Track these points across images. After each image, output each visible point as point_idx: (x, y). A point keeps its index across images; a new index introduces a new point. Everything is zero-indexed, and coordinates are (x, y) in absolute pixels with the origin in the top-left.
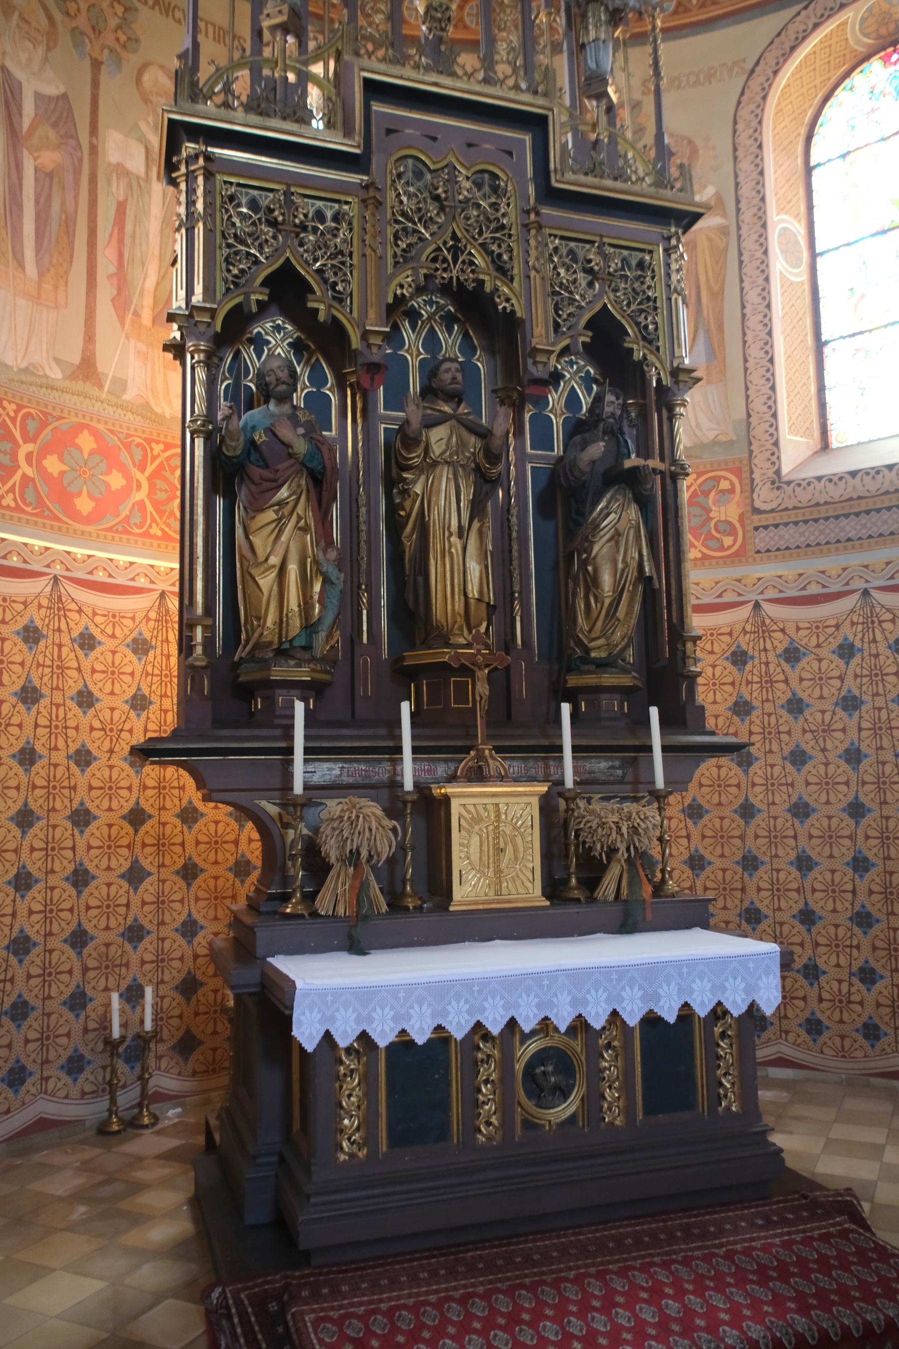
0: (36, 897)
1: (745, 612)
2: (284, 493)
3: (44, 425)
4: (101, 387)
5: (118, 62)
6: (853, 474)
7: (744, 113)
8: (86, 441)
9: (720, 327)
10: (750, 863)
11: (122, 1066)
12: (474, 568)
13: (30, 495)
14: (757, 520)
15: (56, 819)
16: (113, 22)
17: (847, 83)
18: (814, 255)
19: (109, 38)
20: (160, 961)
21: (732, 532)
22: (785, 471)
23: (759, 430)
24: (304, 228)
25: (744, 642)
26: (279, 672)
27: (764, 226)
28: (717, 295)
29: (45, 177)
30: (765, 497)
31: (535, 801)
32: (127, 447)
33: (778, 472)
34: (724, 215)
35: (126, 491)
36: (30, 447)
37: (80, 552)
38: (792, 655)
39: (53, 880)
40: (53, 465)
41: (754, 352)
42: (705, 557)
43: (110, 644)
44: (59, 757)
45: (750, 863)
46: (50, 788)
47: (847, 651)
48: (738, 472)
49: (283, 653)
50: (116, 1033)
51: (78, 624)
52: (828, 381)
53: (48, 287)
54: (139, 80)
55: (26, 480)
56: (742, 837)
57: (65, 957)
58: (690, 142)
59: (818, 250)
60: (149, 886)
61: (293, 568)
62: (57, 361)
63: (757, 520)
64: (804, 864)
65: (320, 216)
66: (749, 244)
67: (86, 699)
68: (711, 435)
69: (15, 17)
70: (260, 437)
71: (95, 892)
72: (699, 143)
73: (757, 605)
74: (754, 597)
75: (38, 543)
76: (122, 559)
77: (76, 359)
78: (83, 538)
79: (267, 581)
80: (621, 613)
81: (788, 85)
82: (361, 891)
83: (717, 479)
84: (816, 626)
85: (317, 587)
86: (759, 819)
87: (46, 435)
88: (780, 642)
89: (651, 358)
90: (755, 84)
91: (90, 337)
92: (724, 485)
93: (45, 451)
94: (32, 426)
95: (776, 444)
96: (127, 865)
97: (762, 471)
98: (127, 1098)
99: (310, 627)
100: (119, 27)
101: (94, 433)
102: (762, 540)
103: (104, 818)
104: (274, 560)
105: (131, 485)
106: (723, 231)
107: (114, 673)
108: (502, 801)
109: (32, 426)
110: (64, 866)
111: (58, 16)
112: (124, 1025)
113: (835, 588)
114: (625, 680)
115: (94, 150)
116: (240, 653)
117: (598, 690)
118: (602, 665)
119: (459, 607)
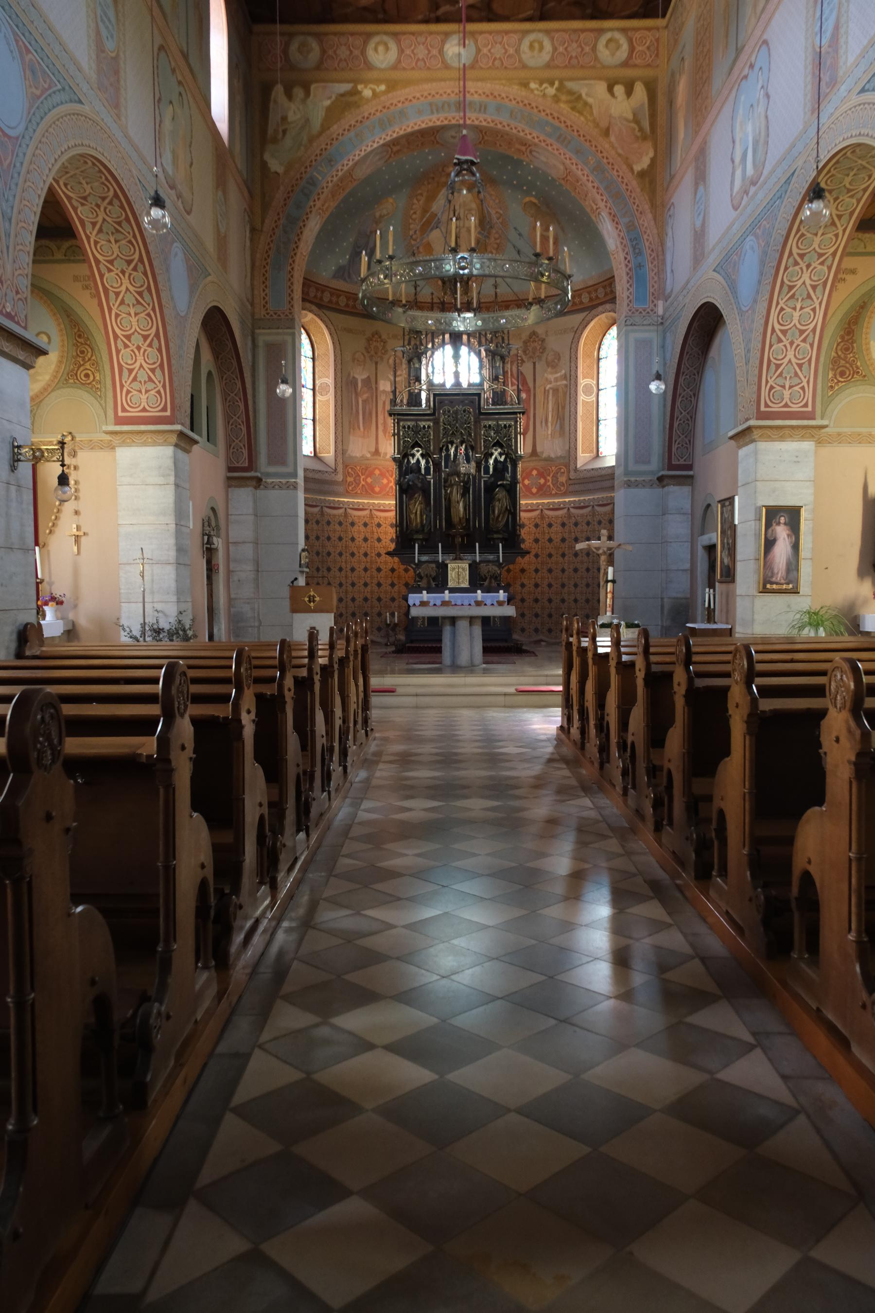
0: (369, 588)
1: (565, 511)
2: (416, 495)
3: (366, 470)
4: (380, 456)
5: (382, 358)
6: (593, 469)
7: (573, 346)
8: (377, 472)
9: (564, 420)
10: (563, 586)
11: (390, 632)
12: (461, 509)
13: (364, 490)
14: (571, 482)
15: (373, 570)
16: (381, 348)
17: (609, 332)
18: (598, 390)
19: (379, 354)
20: (399, 607)
21: (563, 485)
22: (578, 466)
23: (572, 453)
24: (420, 431)
25: (565, 520)
26: (415, 537)
27: (577, 386)
28: (564, 408)
29: (364, 402)
30: (572, 475)
31: (467, 565)
32: (388, 471)
33: (576, 467)
34: (566, 380)
35: (388, 483)
36: (363, 477)
37: (376, 502)
38: (576, 524)
39: (373, 585)
40: (369, 480)
41: (572, 428)
42: (556, 493)
43: (384, 525)
44: (373, 555)
45: (563, 586)
46: (371, 562)
47: (588, 523)
48: (566, 467)
49: (417, 532)
50: (388, 622)
51: (376, 521)
52: (600, 433)
53: (366, 432)
54: (388, 362)
55: (363, 485)
56: (562, 578)
57: (376, 603)
58: (559, 354)
59: (600, 387)
60: (396, 587)
61: (418, 512)
62: (369, 452)
63: (571, 482)
64: (576, 586)
65: (424, 427)
66: (572, 392)
67: (379, 540)
68: (560, 454)
69: (356, 361)
70: (410, 483)
71: (383, 588)
72: (561, 355)
73: (569, 509)
74: (567, 506)
75: (366, 501)
76: (387, 502)
77: (373, 450)
78: (377, 499)
79: (413, 516)
80: (500, 520)
81: (587, 336)
82: (429, 583)
83: (561, 469)
84: (582, 515)
85: (425, 517)
86: (566, 573)
87: (367, 472)
88: (573, 520)
89: (510, 452)
90: (577, 335)
91: (377, 443)
92: (562, 470)
93: (366, 478)
94: (364, 471)
95: (576, 458)
96: (390, 582)
97: (572, 467)
98: (392, 639)
99: (423, 526)
100: (382, 349)
101: (379, 470)
102: (571, 488)
103: (384, 570)
104: (414, 511)
105: (389, 481)
106: (566, 386)
107: (386, 533)
108: (460, 565)
109: (364, 471)
110: (375, 581)
111: (366, 354)
112: (390, 622)
113: (586, 505)
114: (500, 536)
115: (376, 389)
116: (409, 531)
117: (494, 539)
118: (497, 532)
119: (458, 520)
